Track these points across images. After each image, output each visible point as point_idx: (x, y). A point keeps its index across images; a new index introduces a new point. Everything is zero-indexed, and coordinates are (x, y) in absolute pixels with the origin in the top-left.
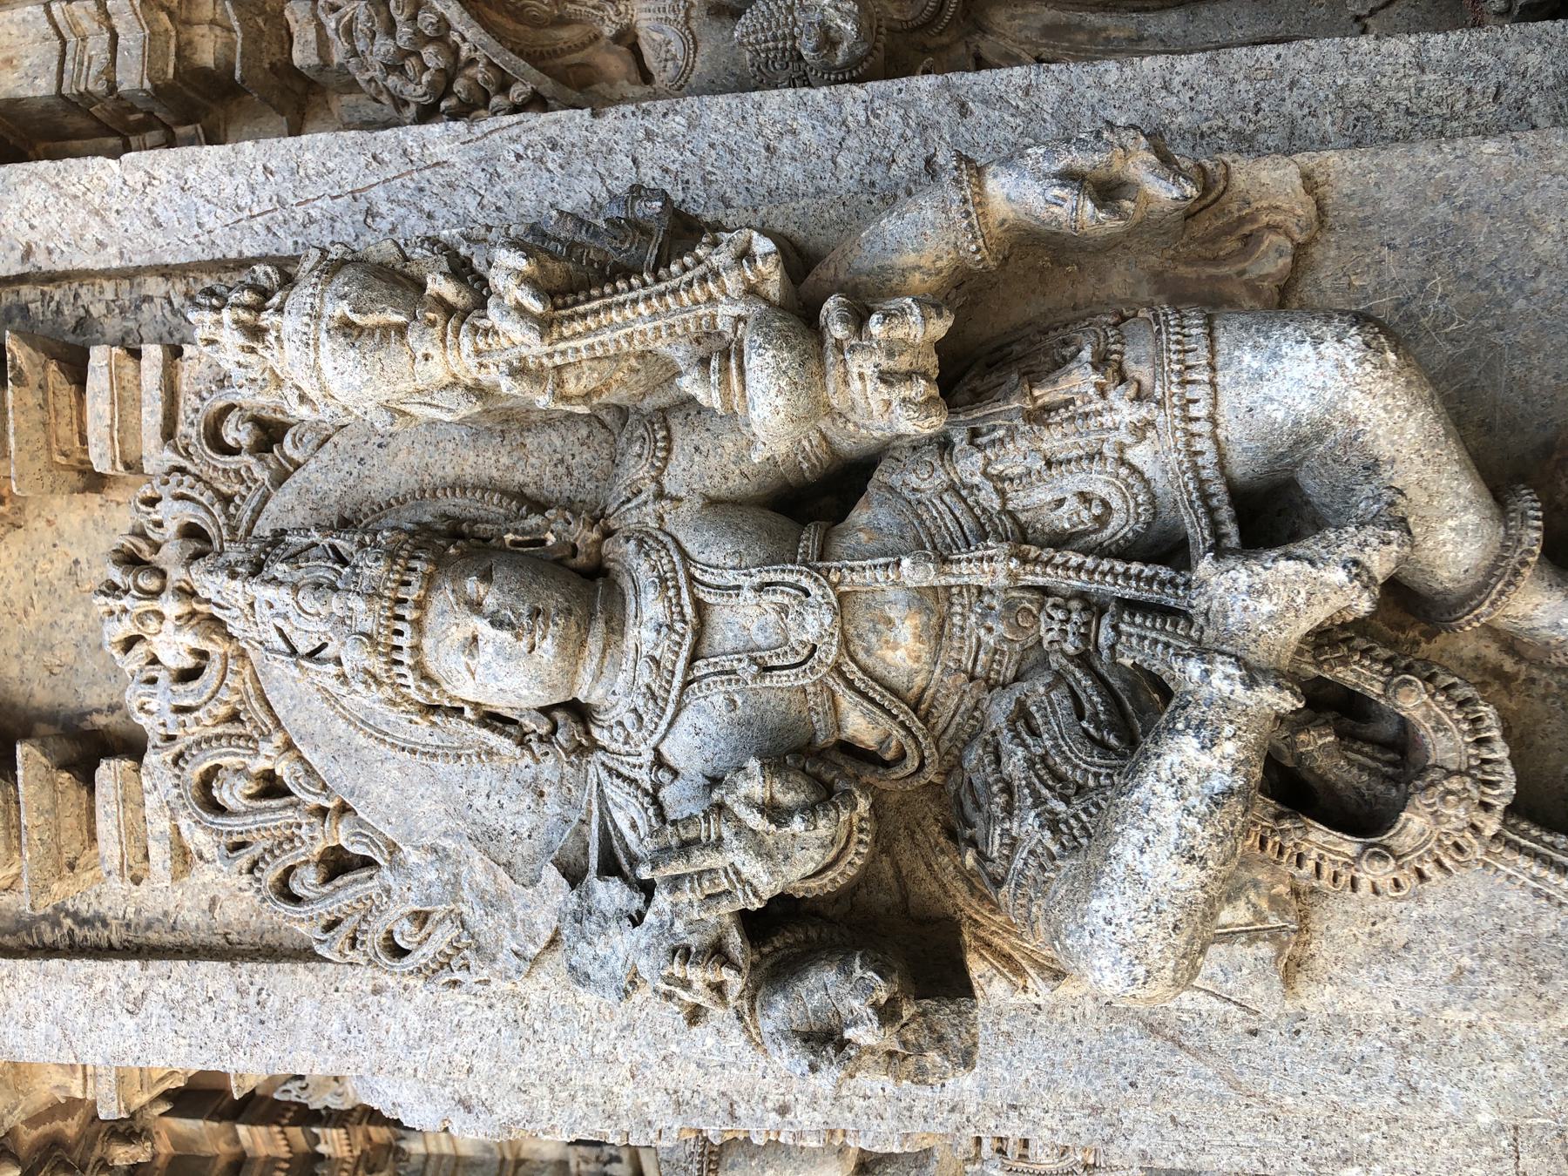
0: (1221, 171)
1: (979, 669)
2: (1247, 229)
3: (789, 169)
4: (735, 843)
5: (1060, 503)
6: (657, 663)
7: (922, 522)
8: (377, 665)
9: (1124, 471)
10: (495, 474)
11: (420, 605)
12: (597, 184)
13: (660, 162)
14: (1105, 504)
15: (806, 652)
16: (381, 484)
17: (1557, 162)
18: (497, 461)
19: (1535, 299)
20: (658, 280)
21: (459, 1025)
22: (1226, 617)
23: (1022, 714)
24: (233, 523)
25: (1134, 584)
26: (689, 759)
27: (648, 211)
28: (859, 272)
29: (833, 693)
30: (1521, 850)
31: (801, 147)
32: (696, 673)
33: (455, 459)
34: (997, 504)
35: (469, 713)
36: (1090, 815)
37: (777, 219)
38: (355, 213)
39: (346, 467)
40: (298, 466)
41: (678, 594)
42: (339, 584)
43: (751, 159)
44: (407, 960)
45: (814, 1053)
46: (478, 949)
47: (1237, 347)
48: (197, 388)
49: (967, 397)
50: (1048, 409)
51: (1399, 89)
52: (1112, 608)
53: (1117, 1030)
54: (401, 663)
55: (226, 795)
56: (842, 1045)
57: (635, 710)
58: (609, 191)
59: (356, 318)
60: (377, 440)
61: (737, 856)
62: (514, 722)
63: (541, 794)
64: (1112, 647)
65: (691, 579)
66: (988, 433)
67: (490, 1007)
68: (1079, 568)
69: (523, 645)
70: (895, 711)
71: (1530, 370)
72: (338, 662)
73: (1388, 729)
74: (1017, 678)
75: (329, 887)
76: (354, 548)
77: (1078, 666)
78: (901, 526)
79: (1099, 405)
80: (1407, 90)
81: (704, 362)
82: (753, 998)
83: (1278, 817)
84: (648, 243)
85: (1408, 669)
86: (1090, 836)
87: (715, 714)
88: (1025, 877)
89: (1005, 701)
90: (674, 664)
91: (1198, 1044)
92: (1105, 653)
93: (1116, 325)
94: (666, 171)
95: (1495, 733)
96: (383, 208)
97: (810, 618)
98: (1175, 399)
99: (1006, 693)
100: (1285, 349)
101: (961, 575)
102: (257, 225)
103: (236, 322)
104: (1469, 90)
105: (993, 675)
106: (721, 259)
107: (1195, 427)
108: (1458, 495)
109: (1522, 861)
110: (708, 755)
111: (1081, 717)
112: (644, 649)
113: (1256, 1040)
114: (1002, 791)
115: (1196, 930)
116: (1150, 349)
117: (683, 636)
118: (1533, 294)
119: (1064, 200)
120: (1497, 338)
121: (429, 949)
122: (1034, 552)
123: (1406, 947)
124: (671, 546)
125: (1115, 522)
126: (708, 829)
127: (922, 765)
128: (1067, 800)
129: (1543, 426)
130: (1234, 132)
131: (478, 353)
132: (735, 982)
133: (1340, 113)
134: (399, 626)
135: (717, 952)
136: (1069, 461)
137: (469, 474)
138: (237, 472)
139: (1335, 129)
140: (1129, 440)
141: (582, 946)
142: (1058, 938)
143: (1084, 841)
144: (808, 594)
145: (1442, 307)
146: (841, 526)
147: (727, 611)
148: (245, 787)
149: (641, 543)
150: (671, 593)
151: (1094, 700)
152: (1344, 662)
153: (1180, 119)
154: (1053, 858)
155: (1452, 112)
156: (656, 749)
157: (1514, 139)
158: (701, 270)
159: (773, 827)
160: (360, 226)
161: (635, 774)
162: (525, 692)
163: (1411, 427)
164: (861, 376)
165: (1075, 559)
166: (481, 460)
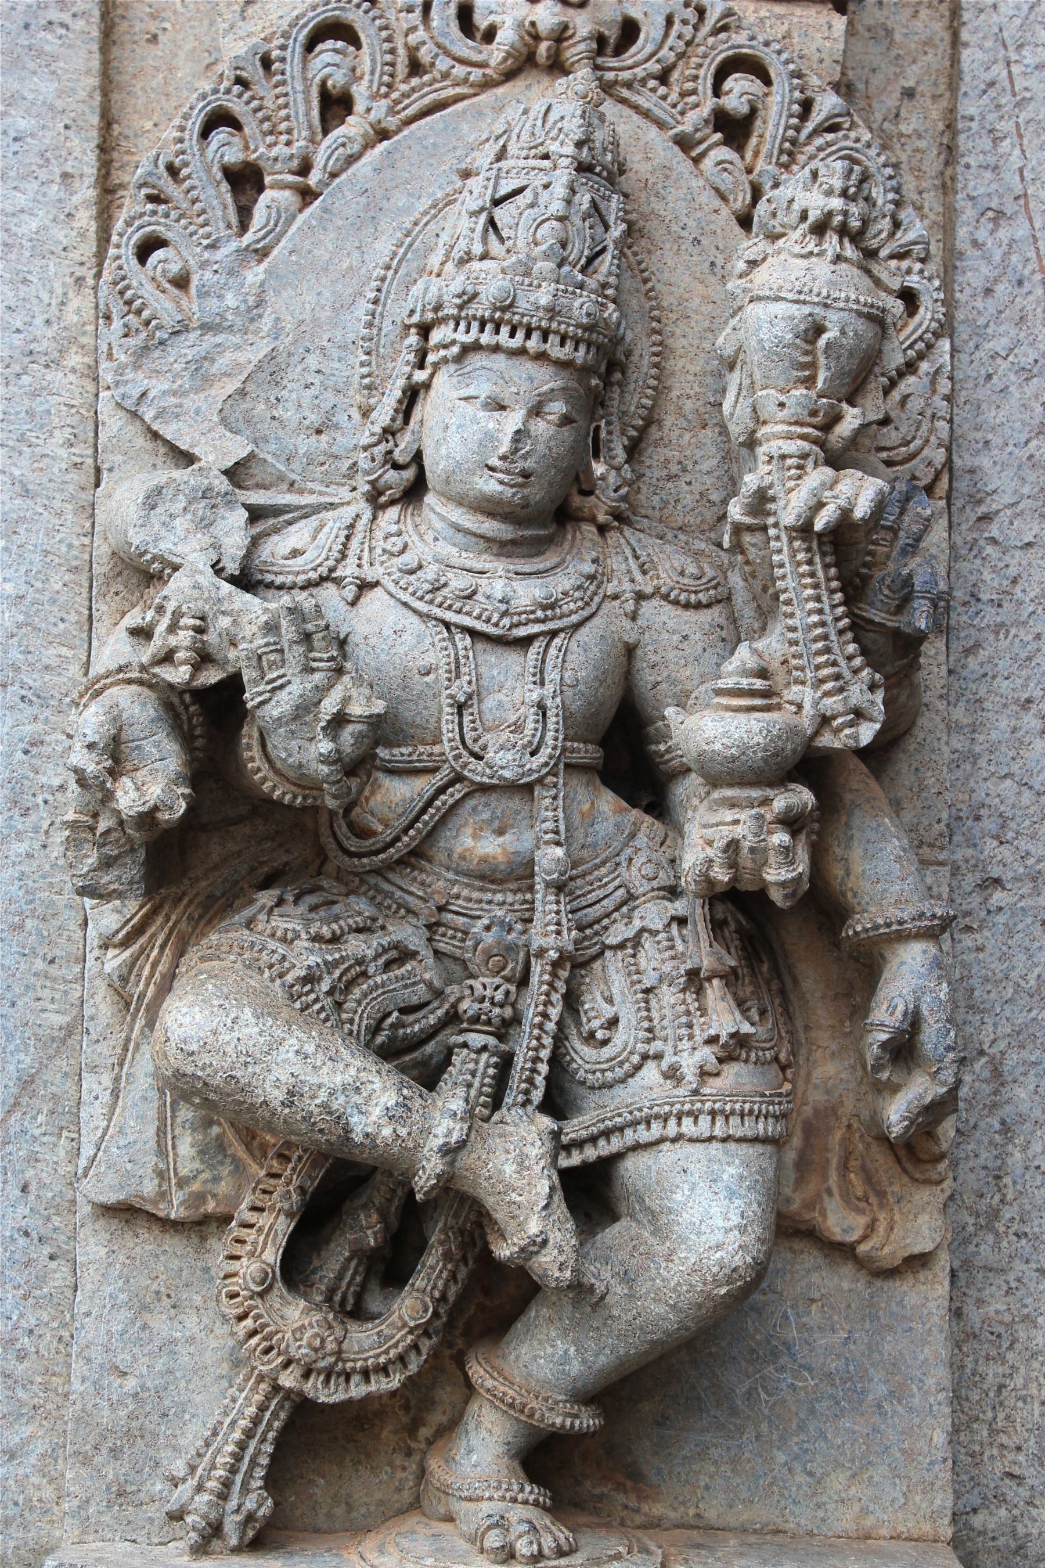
0: (935, 1177)
1: (450, 916)
2: (873, 1199)
3: (1004, 723)
4: (309, 686)
5: (610, 1001)
6: (469, 597)
7: (597, 867)
8: (480, 309)
9: (636, 1059)
10: (675, 393)
11: (541, 357)
12: (1007, 499)
13: (1025, 576)
14: (605, 1042)
15: (477, 749)
16: (670, 263)
17: (918, 1498)
18: (689, 397)
19: (785, 1470)
20: (841, 632)
21: (25, 281)
22: (501, 1136)
23: (403, 955)
24: (636, 85)
25: (529, 1065)
26: (369, 620)
27: (917, 613)
28: (850, 814)
29: (434, 770)
30: (262, 1409)
31: (1027, 739)
32: (458, 637)
33: (693, 350)
34: (612, 940)
35: (420, 376)
36: (319, 1012)
37: (931, 720)
38: (1001, 197)
39: (691, 223)
40: (697, 161)
41: (537, 621)
42: (566, 269)
43: (1019, 682)
44: (134, 262)
45: (107, 746)
46: (146, 348)
47: (742, 1162)
48: (795, 34)
49: (720, 916)
50: (700, 991)
51: (1027, 1380)
52: (503, 1047)
53: (27, 1045)
54: (482, 330)
55: (327, 57)
56: (114, 773)
57: (420, 567)
58: (998, 512)
59: (822, 342)
60: (720, 262)
61: (297, 688)
62: (406, 420)
63: (319, 432)
64: (465, 1045)
65: (554, 634)
66: (681, 934)
67: (48, 322)
68: (545, 1016)
69: (495, 462)
70: (412, 832)
71: (715, 1463)
72: (484, 257)
73: (374, 1304)
74: (436, 952)
75: (219, 175)
76: (601, 279)
77: (447, 1013)
78: (594, 846)
79: (699, 1038)
80: (1025, 1387)
81: (763, 673)
82: (141, 682)
83: (302, 1190)
84: (888, 612)
85: (436, 1314)
86: (302, 1010)
87: (416, 653)
88: (260, 951)
89: (416, 940)
90: (468, 614)
91: (12, 1131)
92: (460, 1039)
93: (776, 1059)
94: (1015, 581)
95: (373, 1387)
96: (1004, 234)
97: (509, 756)
98: (699, 1105)
99: (423, 942)
100: (738, 1202)
101: (545, 903)
102: (999, 71)
103: (830, 214)
104: (1019, 1449)
105: (442, 930)
106: (857, 694)
107: (672, 1122)
108: (597, 1355)
109: (252, 1410)
110: (373, 641)
111: (404, 1011)
112: (483, 581)
113: (18, 1193)
114: (334, 933)
115: (229, 1095)
116: (747, 1088)
117: (496, 625)
118: (790, 1470)
119: (892, 1014)
120: (749, 1434)
121: (148, 291)
122: (564, 974)
123: (145, 1327)
124: (585, 613)
125: (588, 1052)
126: (321, 660)
127: (351, 854)
128: (330, 993)
129: (659, 1471)
130: (999, 1211)
131: (783, 457)
132: (178, 674)
133: (1008, 1318)
134: (520, 335)
135: (204, 658)
136: (648, 1010)
137: (676, 364)
138: (694, 92)
139: (992, 1314)
140: (665, 1064)
141: (181, 502)
142: (210, 977)
143: (298, 1005)
144: (532, 754)
145: (783, 1386)
146: (598, 782)
147: (519, 669)
148: (337, 80)
149: (591, 578)
150: (540, 614)
151: (415, 1027)
152: (447, 1256)
153: (1018, 1155)
154: (281, 976)
155: (998, 1432)
156: (377, 583)
157: (945, 1460)
158: (847, 674)
159: (323, 724)
160: (985, 203)
161: (352, 560)
162: (443, 451)
163: (660, 1309)
164: (736, 822)
165: (554, 1012)
166: (690, 378)
